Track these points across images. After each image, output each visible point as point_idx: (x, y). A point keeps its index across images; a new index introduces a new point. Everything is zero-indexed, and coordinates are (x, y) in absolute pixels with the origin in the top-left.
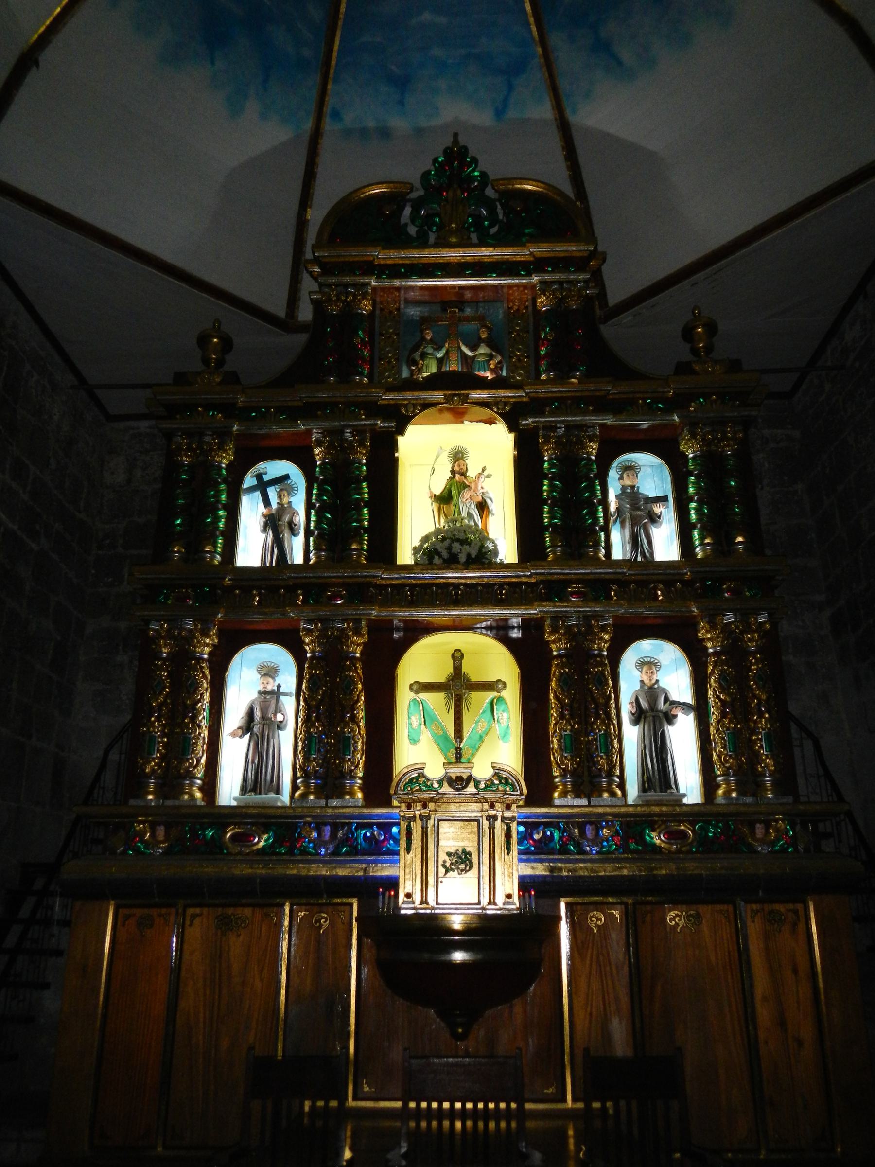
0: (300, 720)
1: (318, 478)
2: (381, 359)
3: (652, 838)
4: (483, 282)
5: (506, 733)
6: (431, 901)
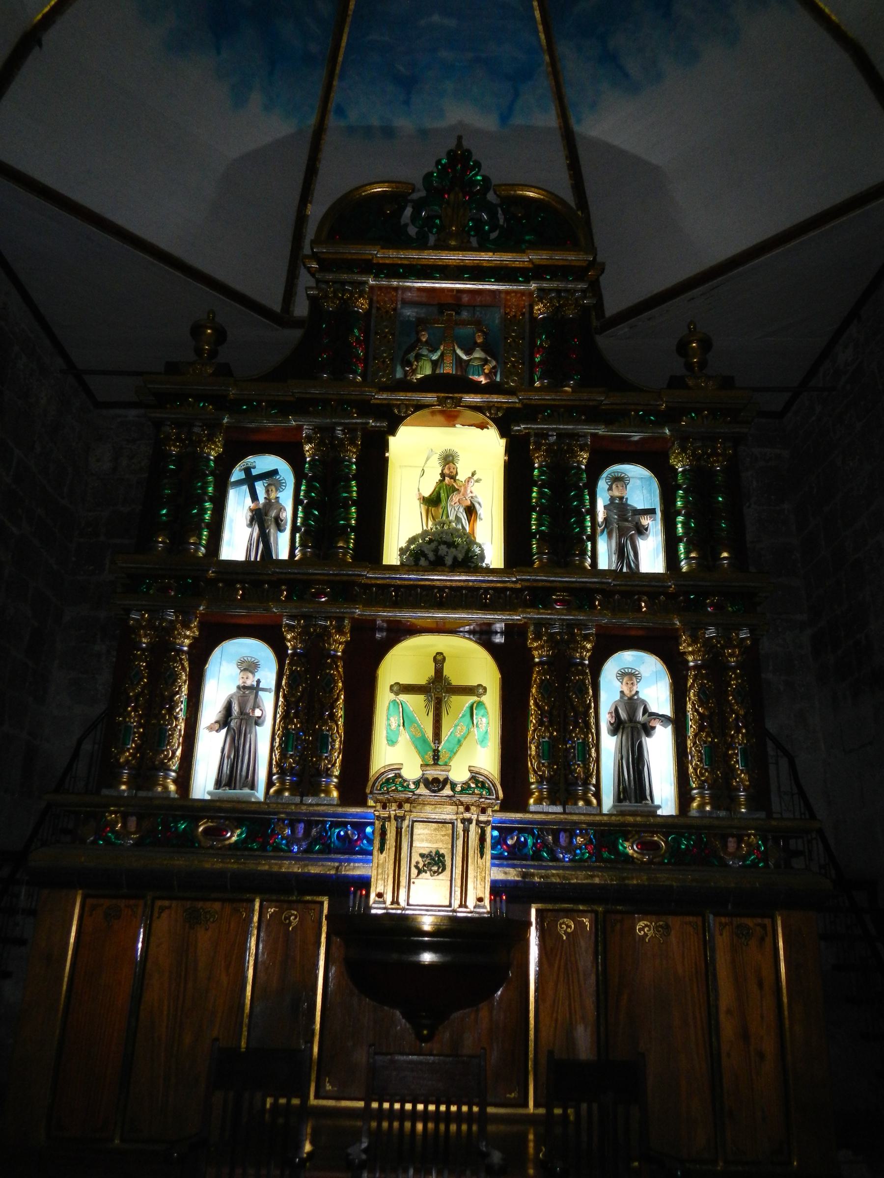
0: (278, 716)
1: (307, 474)
2: (375, 359)
3: (625, 848)
4: (481, 287)
5: (485, 738)
6: (403, 903)
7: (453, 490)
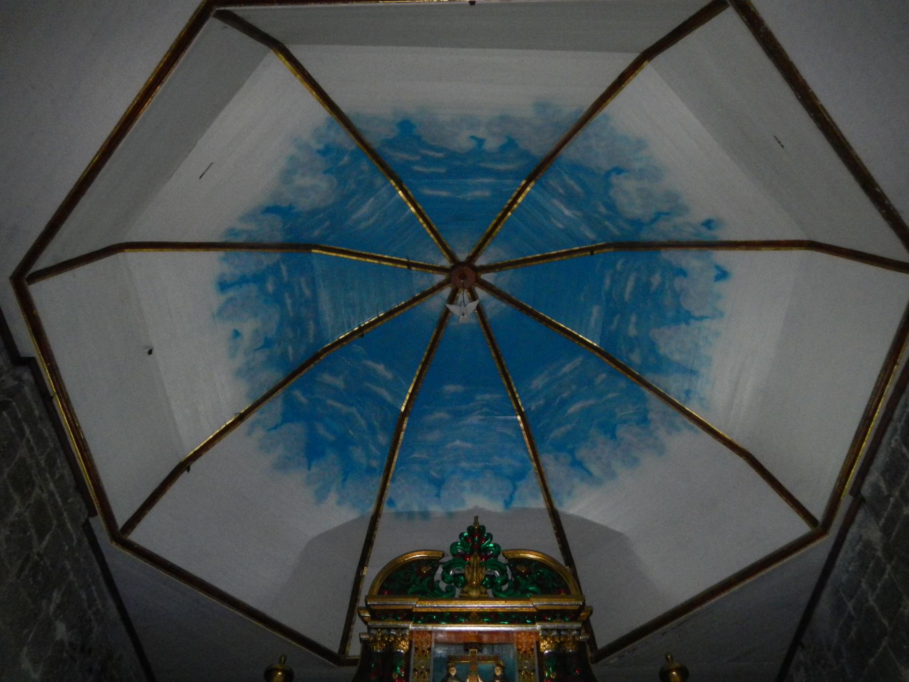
4: (497, 629)
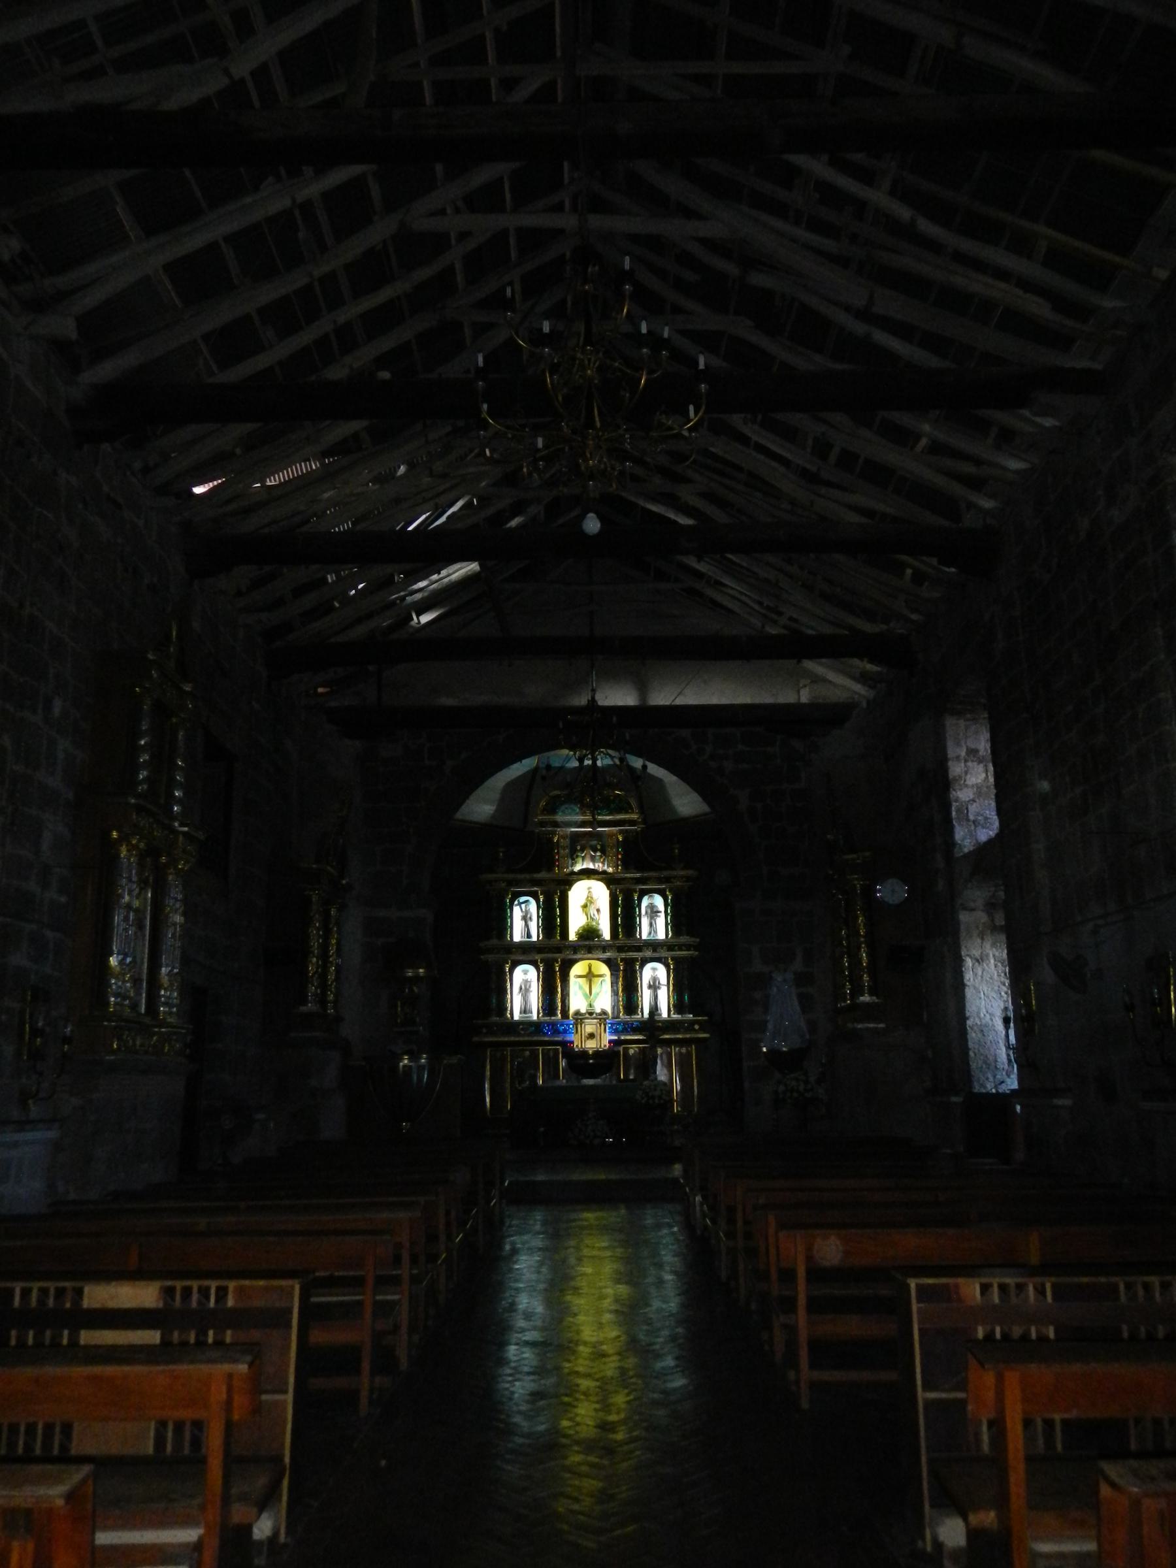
6: (583, 1047)
7: (591, 903)
